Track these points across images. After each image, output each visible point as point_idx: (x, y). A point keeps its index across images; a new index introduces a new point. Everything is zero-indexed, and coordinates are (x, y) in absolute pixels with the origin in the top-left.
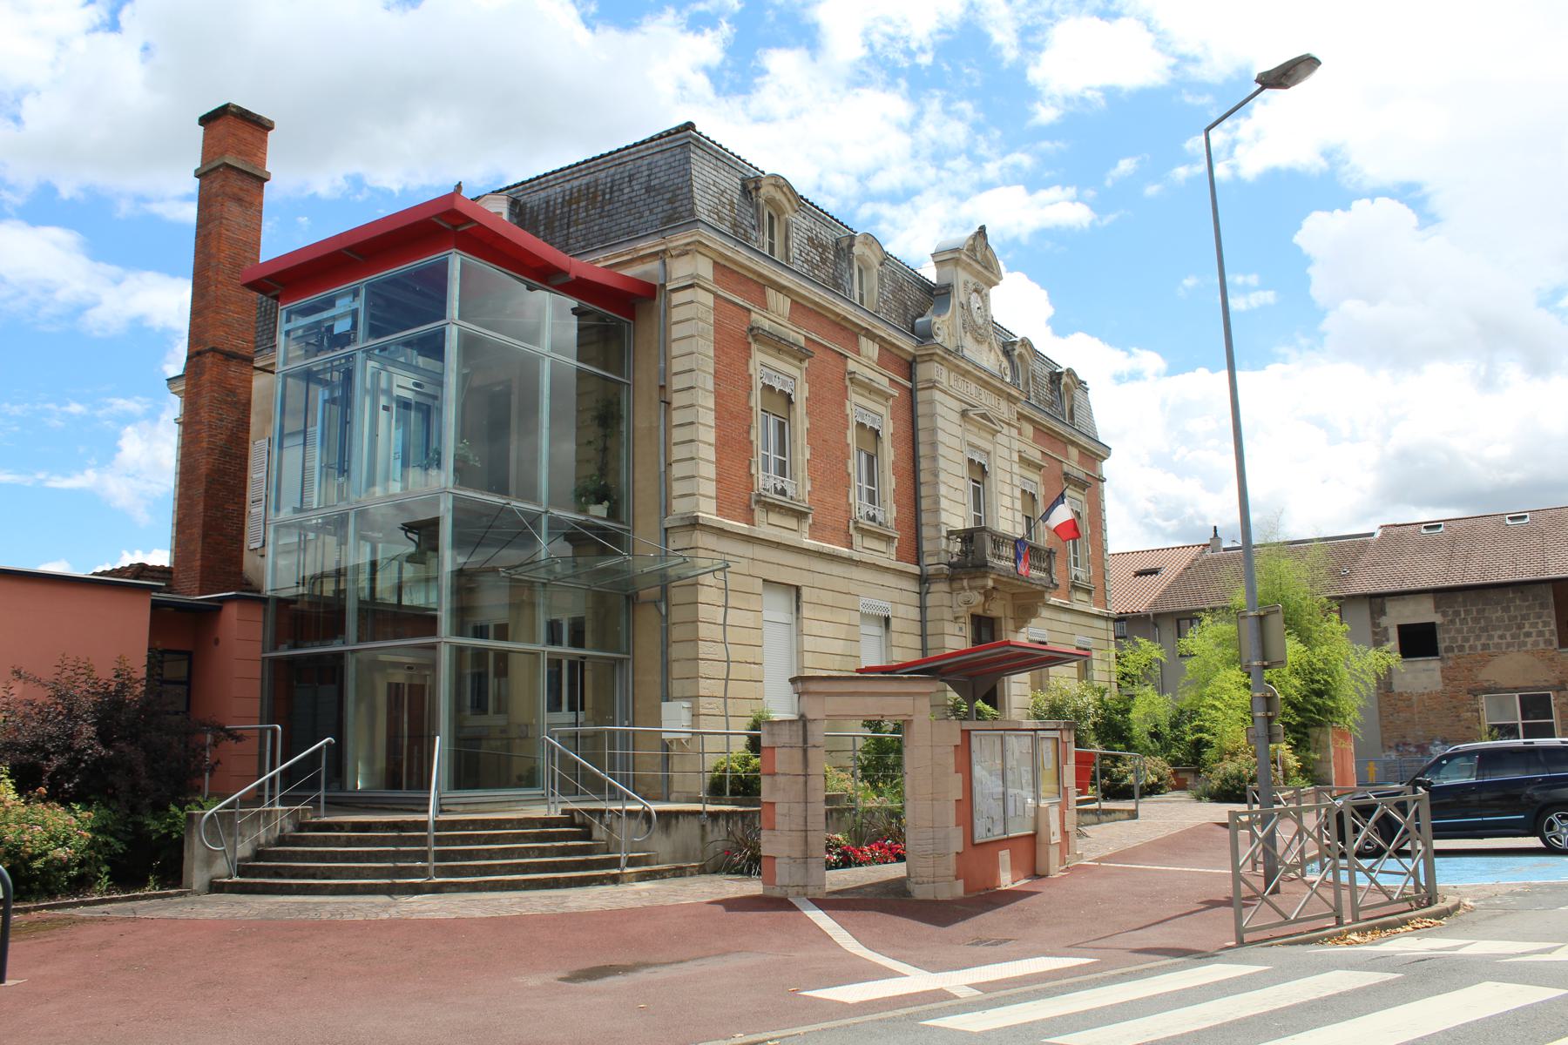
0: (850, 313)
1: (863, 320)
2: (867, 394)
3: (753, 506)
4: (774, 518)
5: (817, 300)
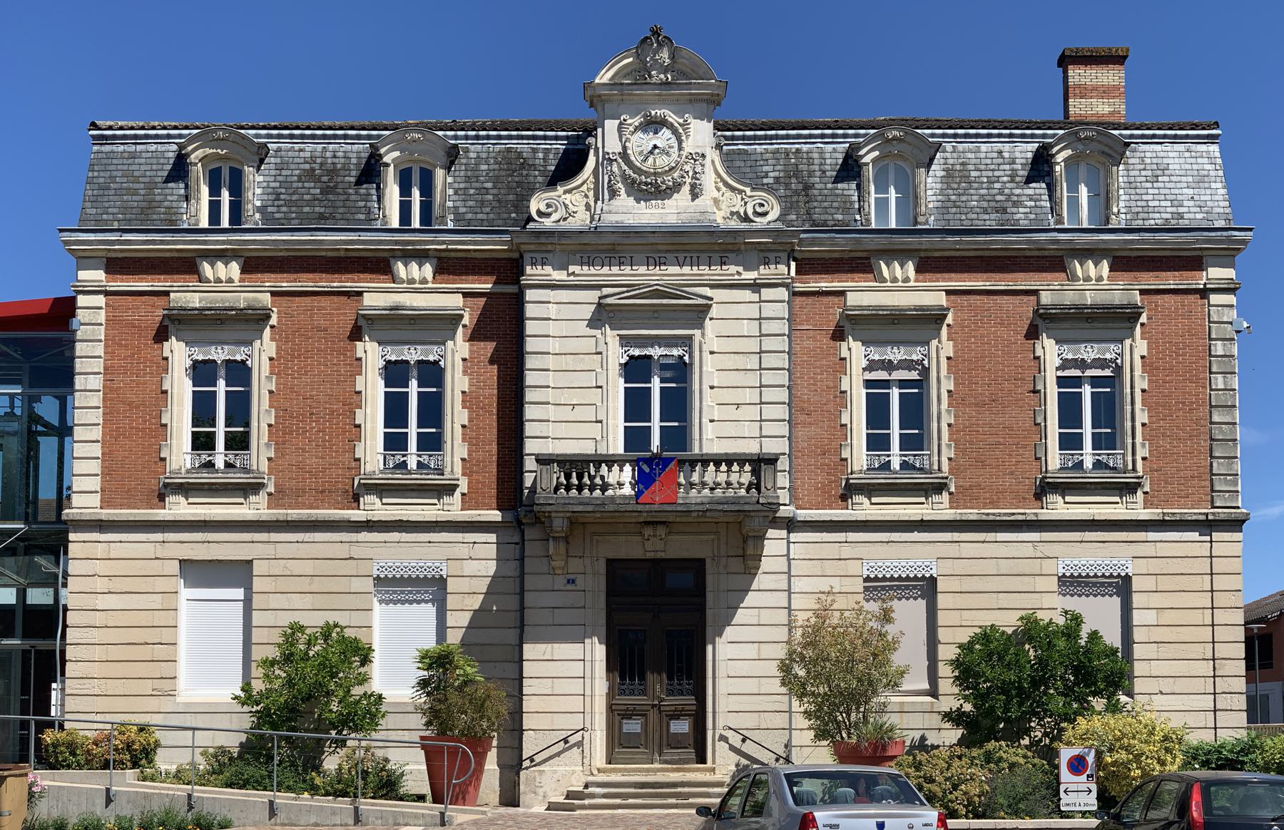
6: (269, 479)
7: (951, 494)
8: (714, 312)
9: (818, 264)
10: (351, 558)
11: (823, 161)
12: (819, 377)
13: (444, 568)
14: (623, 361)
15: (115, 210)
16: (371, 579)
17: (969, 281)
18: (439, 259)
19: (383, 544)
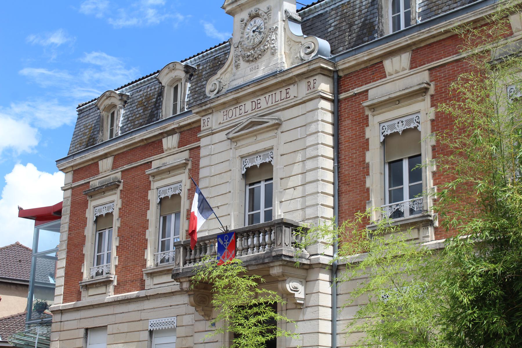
0: (145, 134)
1: (155, 131)
2: (167, 176)
3: (81, 290)
4: (92, 292)
5: (122, 145)
6: (115, 277)
7: (436, 229)
8: (285, 126)
9: (354, 76)
10: (141, 320)
11: (361, 4)
12: (354, 155)
13: (175, 321)
14: (243, 172)
15: (78, 146)
17: (445, 57)
18: (181, 132)
19: (152, 310)
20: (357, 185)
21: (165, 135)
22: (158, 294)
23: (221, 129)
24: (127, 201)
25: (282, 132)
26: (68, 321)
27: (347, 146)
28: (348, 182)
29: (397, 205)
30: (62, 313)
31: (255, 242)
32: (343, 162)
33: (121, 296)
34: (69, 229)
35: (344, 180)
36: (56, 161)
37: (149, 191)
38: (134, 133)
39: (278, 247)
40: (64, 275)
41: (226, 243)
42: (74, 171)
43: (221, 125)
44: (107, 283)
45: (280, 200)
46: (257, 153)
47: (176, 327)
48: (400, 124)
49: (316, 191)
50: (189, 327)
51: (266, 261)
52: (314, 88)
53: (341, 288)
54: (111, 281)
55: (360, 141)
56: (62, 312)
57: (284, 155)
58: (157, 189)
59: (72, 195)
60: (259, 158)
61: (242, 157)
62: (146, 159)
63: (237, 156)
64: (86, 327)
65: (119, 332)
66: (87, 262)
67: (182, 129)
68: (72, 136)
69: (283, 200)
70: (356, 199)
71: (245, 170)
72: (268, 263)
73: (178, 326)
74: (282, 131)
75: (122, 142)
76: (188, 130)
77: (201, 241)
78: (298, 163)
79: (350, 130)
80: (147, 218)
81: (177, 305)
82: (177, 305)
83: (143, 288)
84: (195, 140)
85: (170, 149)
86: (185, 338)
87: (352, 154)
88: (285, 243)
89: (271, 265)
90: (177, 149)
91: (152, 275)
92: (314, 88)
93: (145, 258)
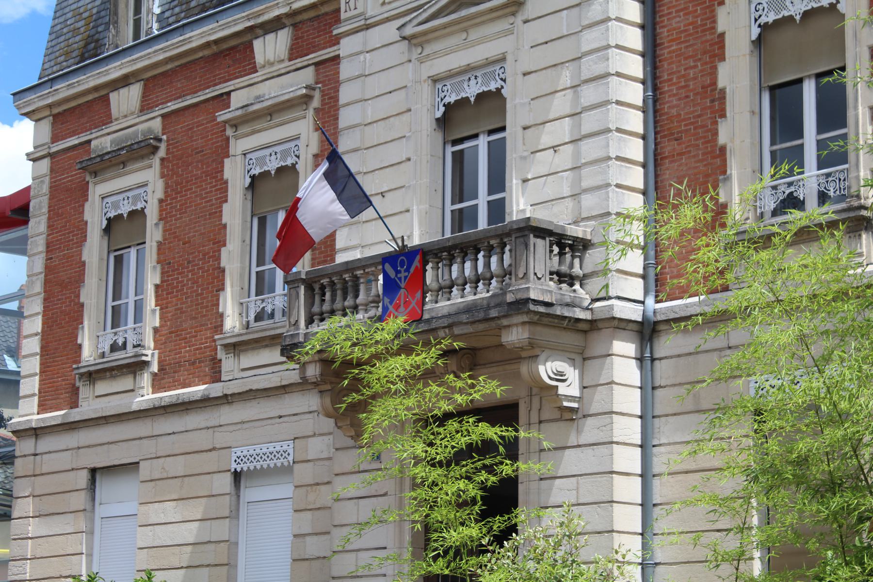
0: (214, 31)
1: (236, 22)
2: (265, 125)
3: (77, 384)
4: (102, 387)
5: (161, 57)
6: (153, 355)
10: (214, 449)
12: (691, 72)
13: (291, 451)
14: (439, 114)
15: (62, 58)
16: (229, 473)
18: (294, 25)
19: (239, 426)
20: (697, 139)
21: (259, 31)
22: (251, 390)
23: (386, 15)
24: (177, 184)
25: (525, 22)
26: (50, 452)
27: (674, 51)
28: (678, 132)
29: (790, 184)
30: (37, 436)
31: (468, 271)
32: (666, 89)
33: (168, 395)
34: (47, 247)
35: (669, 129)
36: (14, 94)
37: (226, 160)
38: (187, 29)
39: (520, 281)
40: (38, 350)
41: (402, 275)
42: (55, 116)
43: (387, 7)
44: (137, 366)
45: (523, 177)
46: (468, 70)
47: (294, 462)
48: (274, 157)
49: (605, 155)
50: (321, 463)
51: (493, 313)
52: (356, 8)
53: (663, 371)
54: (146, 364)
55: (704, 39)
56: (36, 432)
57: (529, 73)
58: (245, 154)
59: (52, 170)
60: (473, 81)
61: (435, 80)
62: (217, 87)
63: (424, 77)
64: (92, 466)
65: (165, 475)
66: (89, 320)
67: (299, 18)
68: (47, 37)
69: (529, 177)
70: (696, 171)
71: (442, 109)
72: (498, 318)
73: (298, 462)
74: (525, 18)
75: (162, 49)
76: (310, 20)
77: (347, 271)
78: (563, 93)
79: (681, 14)
80: (224, 222)
81: (294, 415)
82: (294, 415)
83: (216, 377)
84: (329, 42)
85: (272, 64)
86: (315, 487)
87: (685, 69)
88: (535, 274)
89: (505, 322)
90: (287, 63)
91: (237, 347)
92: (356, 8)
93: (221, 310)
